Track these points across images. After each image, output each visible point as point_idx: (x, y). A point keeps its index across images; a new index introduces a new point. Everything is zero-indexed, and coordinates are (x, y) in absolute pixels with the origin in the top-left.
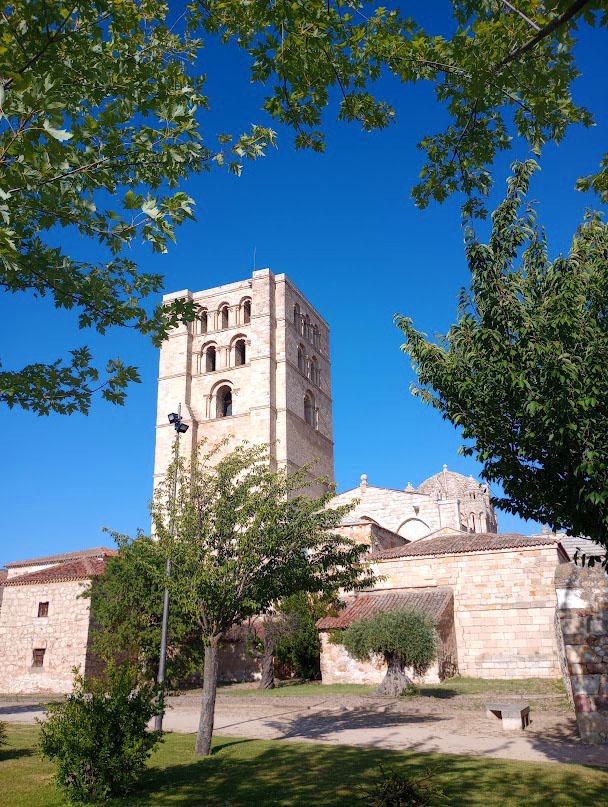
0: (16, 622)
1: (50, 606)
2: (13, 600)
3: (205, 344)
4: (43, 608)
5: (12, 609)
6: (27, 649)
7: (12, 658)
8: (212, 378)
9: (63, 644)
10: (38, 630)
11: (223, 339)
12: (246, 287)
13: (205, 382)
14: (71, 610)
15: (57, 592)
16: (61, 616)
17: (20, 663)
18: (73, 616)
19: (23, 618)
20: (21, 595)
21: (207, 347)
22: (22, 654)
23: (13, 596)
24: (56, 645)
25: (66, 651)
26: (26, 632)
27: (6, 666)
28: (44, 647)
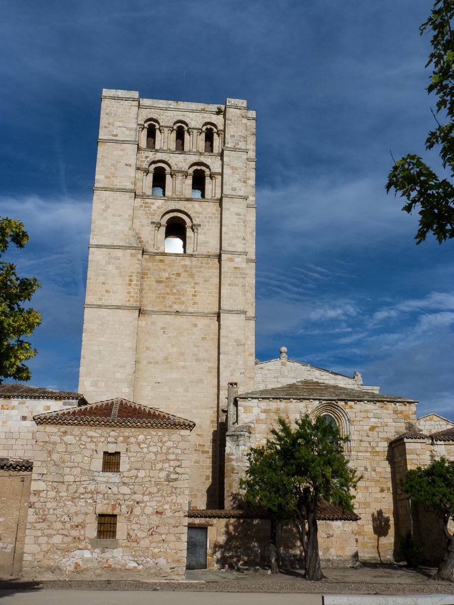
0: (63, 476)
1: (123, 458)
2: (55, 443)
3: (154, 162)
4: (111, 462)
5: (55, 457)
6: (87, 514)
7: (59, 525)
8: (159, 206)
9: (149, 511)
10: (103, 488)
11: (180, 162)
12: (211, 112)
13: (154, 207)
14: (159, 466)
15: (132, 440)
16: (142, 474)
17: (75, 533)
18: (163, 474)
19: (77, 471)
20: (68, 439)
21: (153, 166)
22: (78, 520)
23: (58, 439)
24: (137, 510)
25: (155, 520)
26: (81, 490)
27: (50, 536)
28: (115, 513)
